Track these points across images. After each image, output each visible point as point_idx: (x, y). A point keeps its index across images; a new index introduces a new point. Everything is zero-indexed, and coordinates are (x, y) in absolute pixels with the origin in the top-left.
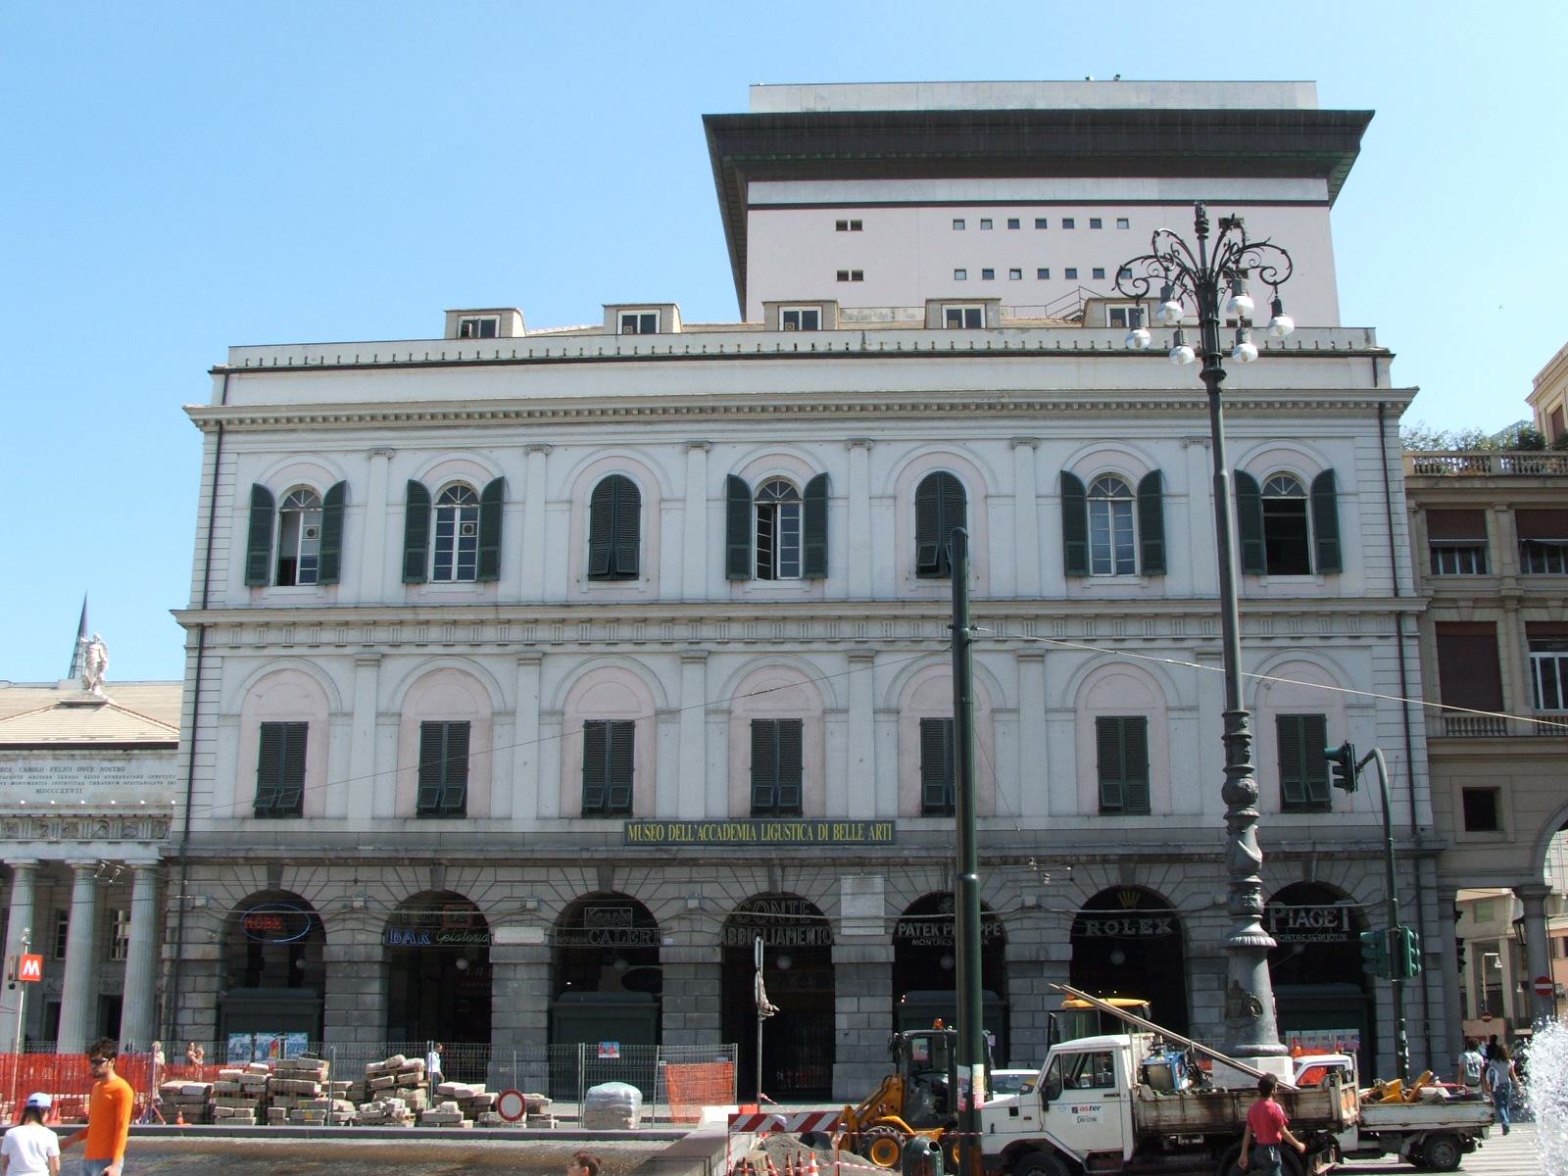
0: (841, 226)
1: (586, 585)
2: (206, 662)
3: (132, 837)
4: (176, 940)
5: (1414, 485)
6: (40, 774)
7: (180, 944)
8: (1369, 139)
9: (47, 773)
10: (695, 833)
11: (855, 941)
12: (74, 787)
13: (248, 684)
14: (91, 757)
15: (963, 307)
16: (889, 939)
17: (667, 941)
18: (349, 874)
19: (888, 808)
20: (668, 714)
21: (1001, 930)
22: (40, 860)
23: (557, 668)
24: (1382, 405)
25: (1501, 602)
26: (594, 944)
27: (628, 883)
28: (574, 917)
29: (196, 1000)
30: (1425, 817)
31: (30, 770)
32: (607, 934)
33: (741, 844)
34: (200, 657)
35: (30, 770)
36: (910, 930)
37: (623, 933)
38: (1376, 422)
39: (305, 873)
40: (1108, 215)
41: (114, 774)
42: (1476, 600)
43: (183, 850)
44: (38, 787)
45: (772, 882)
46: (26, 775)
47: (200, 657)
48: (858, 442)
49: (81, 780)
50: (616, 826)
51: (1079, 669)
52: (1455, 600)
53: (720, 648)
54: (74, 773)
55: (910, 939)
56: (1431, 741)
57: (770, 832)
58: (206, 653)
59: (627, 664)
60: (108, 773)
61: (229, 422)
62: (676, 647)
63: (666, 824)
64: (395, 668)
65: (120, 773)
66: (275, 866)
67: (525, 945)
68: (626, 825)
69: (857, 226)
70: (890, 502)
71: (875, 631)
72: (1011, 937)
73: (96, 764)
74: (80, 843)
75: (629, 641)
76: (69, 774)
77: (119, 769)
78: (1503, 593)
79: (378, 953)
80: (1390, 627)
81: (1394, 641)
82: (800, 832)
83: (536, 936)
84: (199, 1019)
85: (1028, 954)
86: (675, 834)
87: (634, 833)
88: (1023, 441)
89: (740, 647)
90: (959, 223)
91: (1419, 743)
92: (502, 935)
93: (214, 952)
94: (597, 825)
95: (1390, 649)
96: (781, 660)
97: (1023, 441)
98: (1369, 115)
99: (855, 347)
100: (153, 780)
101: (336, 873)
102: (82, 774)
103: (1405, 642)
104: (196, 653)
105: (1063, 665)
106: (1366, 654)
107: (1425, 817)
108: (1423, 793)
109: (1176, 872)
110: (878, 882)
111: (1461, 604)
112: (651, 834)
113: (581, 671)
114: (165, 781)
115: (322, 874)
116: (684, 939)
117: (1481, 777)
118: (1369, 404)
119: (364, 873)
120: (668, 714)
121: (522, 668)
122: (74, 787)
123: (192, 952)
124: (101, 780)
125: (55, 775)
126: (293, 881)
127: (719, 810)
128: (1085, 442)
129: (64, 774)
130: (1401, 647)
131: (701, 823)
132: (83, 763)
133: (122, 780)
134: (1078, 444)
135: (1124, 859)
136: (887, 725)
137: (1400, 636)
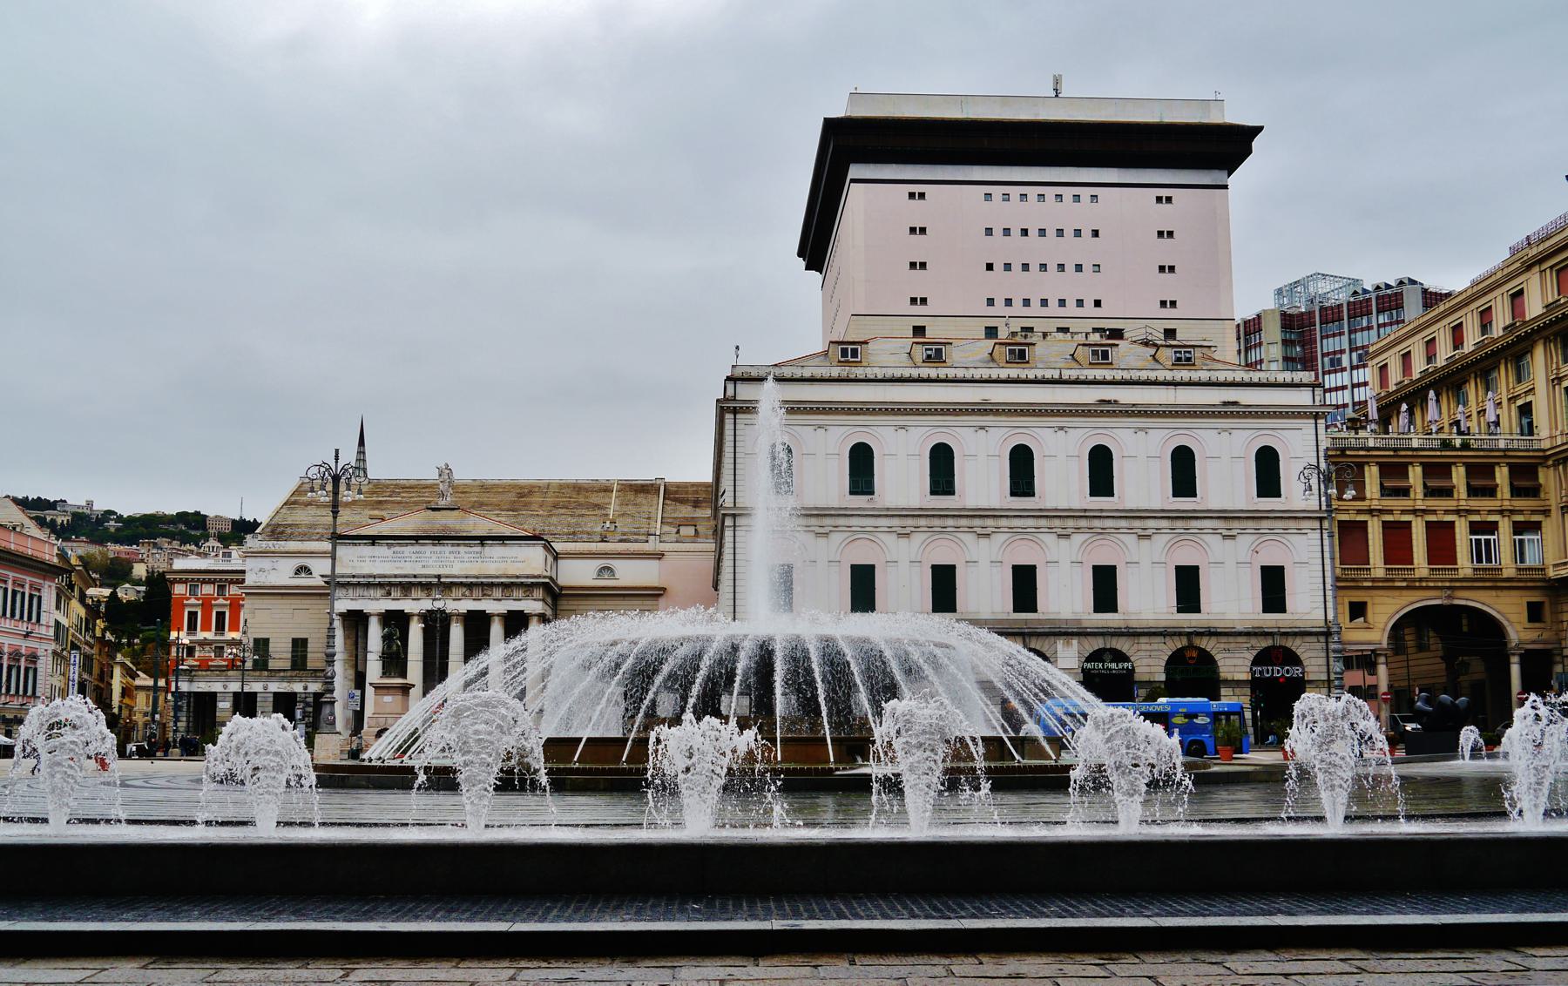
1: (929, 497)
2: (736, 533)
3: (489, 596)
5: (1330, 453)
8: (1257, 143)
14: (458, 545)
16: (1080, 671)
21: (1132, 666)
23: (918, 539)
24: (1317, 413)
25: (1370, 512)
30: (1331, 616)
34: (734, 531)
36: (1089, 666)
38: (1313, 421)
40: (1085, 193)
42: (1358, 510)
47: (734, 531)
48: (1061, 428)
51: (1169, 541)
52: (1348, 510)
53: (996, 530)
54: (447, 555)
56: (1338, 579)
61: (741, 408)
62: (975, 529)
64: (836, 538)
69: (922, 196)
71: (1070, 523)
72: (1136, 671)
73: (462, 549)
74: (454, 600)
77: (477, 553)
78: (1372, 507)
80: (1316, 524)
81: (1319, 531)
85: (1145, 678)
88: (1141, 429)
89: (1006, 530)
90: (988, 196)
91: (1329, 581)
95: (1317, 535)
97: (1141, 429)
98: (1259, 129)
99: (1056, 376)
102: (452, 556)
103: (1324, 531)
105: (1160, 541)
106: (1304, 536)
107: (1331, 616)
108: (1330, 605)
109: (1213, 640)
110: (1075, 642)
111: (1351, 512)
113: (930, 540)
114: (509, 560)
117: (1358, 596)
118: (1311, 413)
121: (900, 539)
124: (466, 560)
127: (998, 609)
128: (1171, 430)
130: (1322, 533)
134: (1167, 431)
135: (1189, 635)
136: (1077, 568)
137: (1321, 529)
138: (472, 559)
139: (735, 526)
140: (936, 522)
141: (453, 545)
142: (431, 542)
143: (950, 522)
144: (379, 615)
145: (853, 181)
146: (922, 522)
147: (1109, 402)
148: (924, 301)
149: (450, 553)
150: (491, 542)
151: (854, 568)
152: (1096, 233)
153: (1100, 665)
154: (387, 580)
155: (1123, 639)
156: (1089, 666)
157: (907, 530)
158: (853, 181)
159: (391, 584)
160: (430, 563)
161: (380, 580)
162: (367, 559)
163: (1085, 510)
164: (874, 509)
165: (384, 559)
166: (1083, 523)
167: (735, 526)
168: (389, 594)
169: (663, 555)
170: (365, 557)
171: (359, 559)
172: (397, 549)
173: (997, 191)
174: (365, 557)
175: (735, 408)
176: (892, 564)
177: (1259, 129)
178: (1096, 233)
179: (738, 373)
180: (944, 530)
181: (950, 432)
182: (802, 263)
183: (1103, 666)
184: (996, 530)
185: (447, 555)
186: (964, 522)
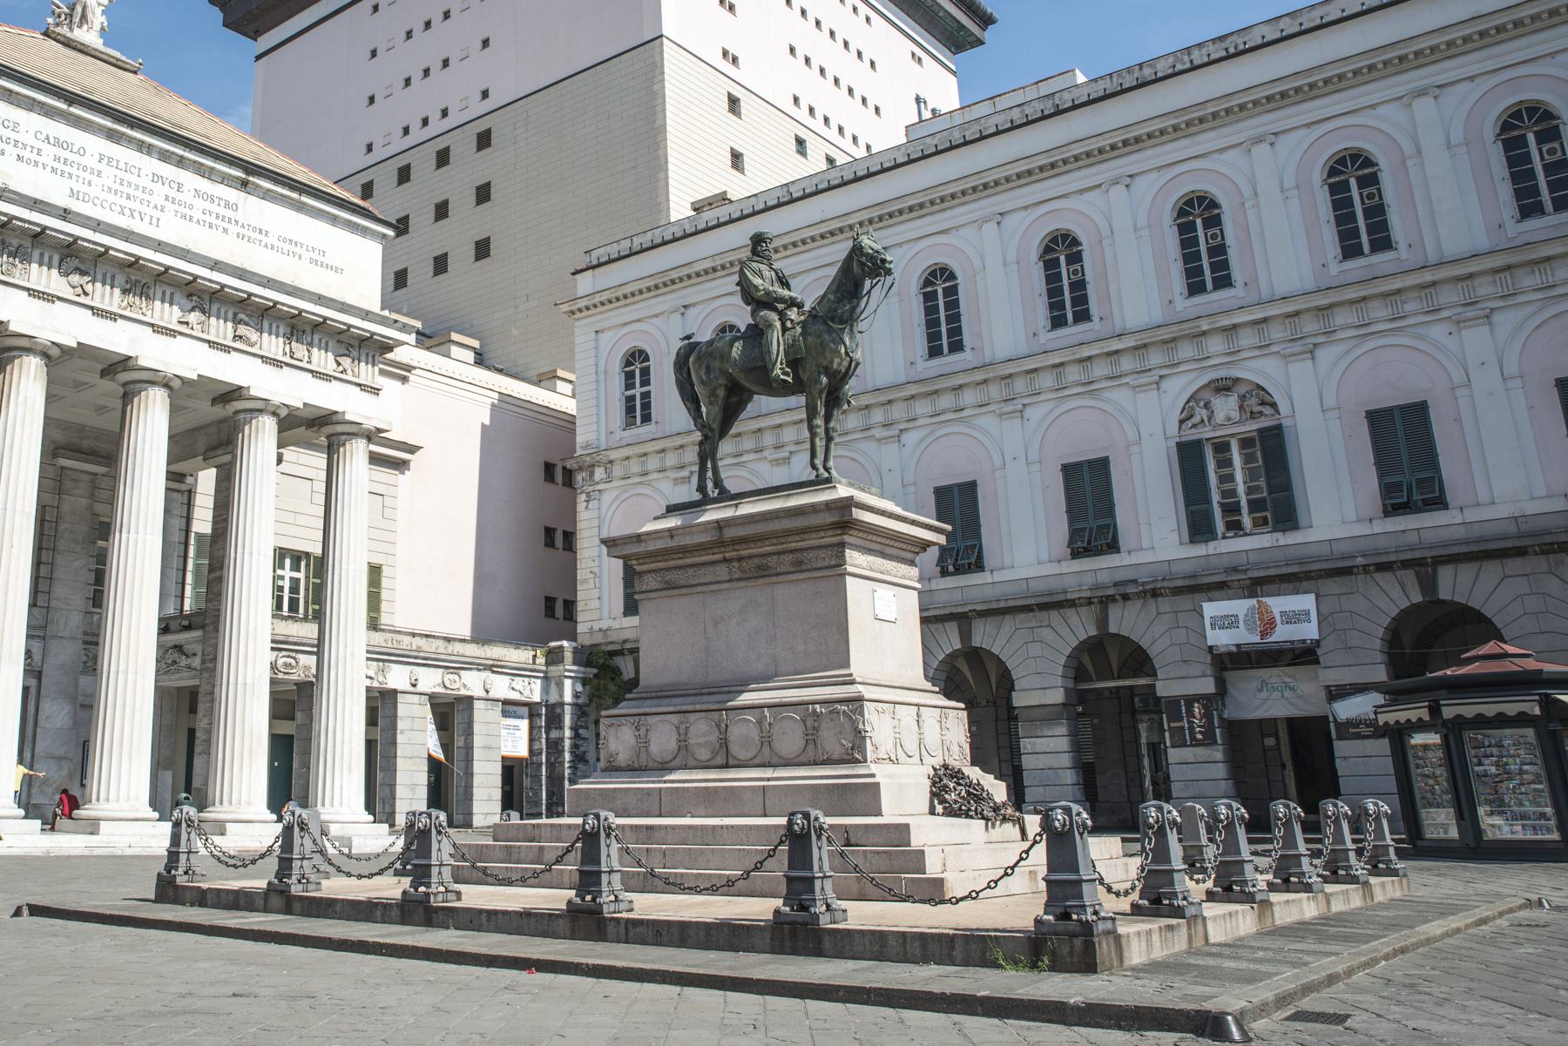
6: (76, 158)
9: (92, 162)
14: (181, 162)
31: (58, 143)
35: (58, 143)
41: (222, 211)
44: (77, 187)
46: (49, 151)
49: (160, 201)
54: (145, 182)
60: (214, 208)
65: (229, 213)
73: (189, 179)
76: (133, 179)
100: (286, 247)
114: (306, 255)
124: (197, 215)
125: (108, 172)
129: (121, 174)
133: (233, 229)
138: (212, 219)
141: (165, 157)
142: (108, 123)
148: (735, 60)
149: (156, 178)
160: (93, 191)
185: (145, 182)
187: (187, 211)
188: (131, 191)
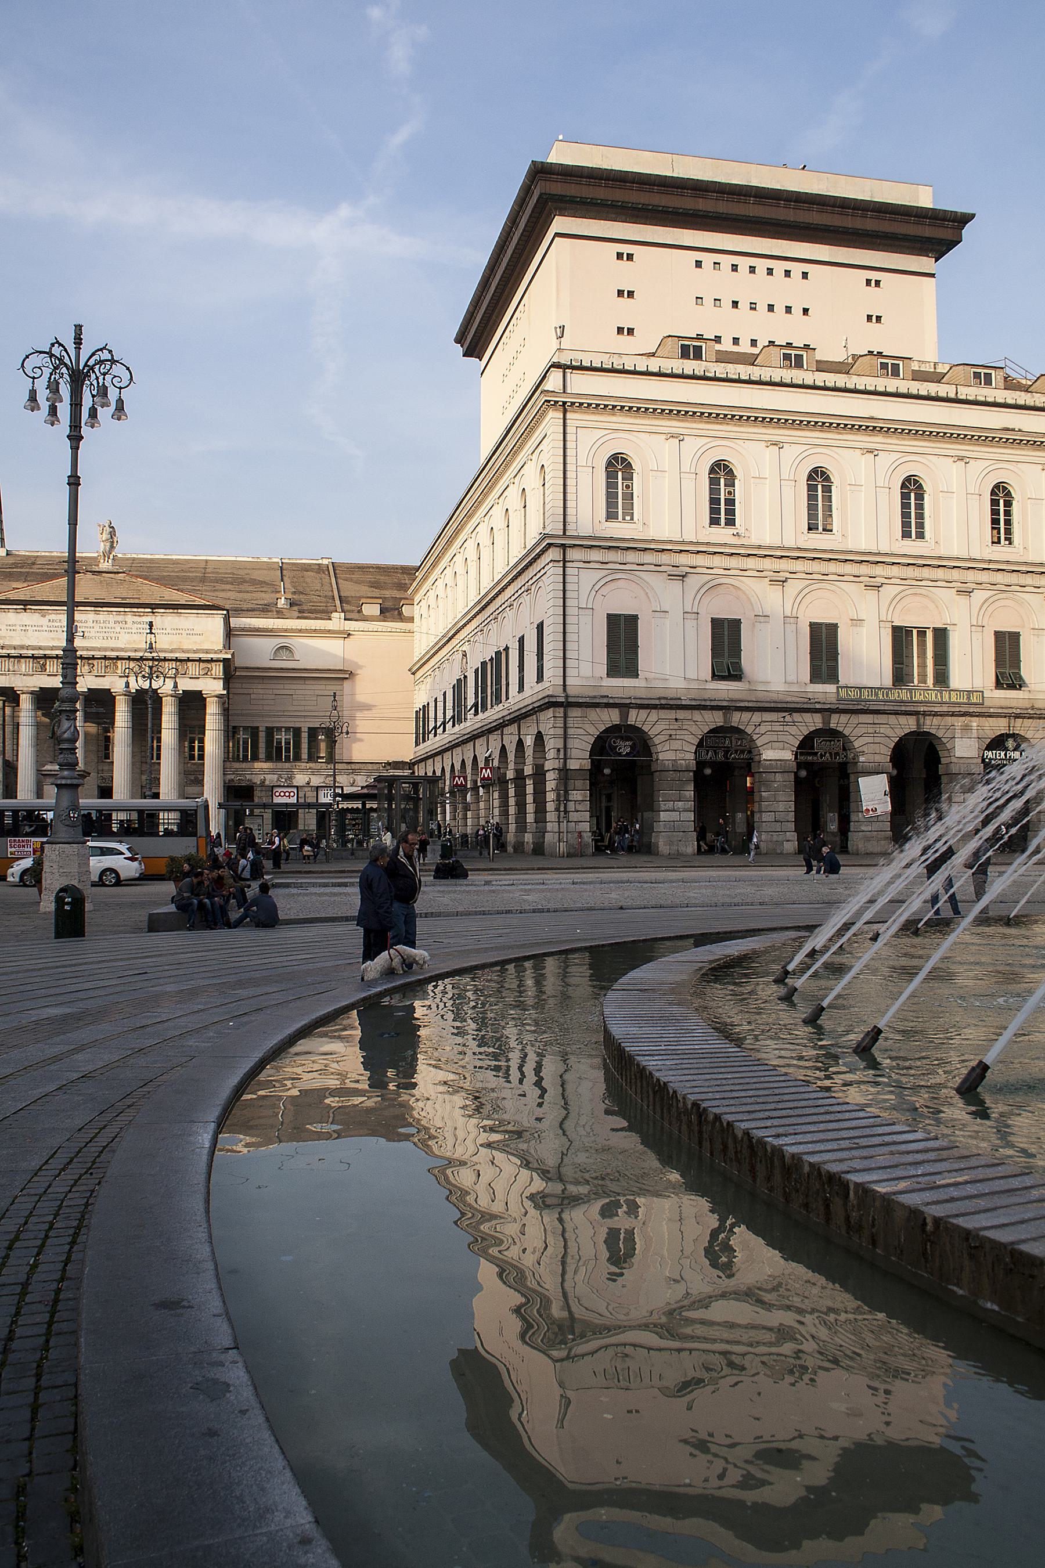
0: (620, 256)
2: (568, 571)
4: (562, 756)
6: (84, 625)
7: (565, 759)
10: (876, 695)
11: (962, 761)
12: (112, 635)
13: (597, 588)
15: (983, 371)
17: (862, 759)
18: (671, 714)
19: (978, 685)
20: (857, 622)
22: (40, 688)
26: (820, 760)
27: (837, 722)
28: (806, 744)
29: (576, 795)
32: (828, 755)
33: (902, 702)
34: (564, 567)
37: (837, 754)
39: (643, 713)
40: (797, 268)
43: (567, 697)
45: (918, 724)
47: (564, 567)
48: (961, 459)
49: (118, 630)
50: (831, 688)
53: (886, 581)
54: (113, 625)
55: (990, 759)
57: (918, 695)
58: (568, 564)
59: (833, 588)
60: (139, 626)
61: (573, 403)
63: (860, 688)
66: (625, 707)
67: (780, 760)
68: (838, 687)
69: (630, 257)
70: (978, 496)
71: (971, 576)
73: (130, 618)
75: (836, 574)
79: (693, 765)
82: (934, 696)
83: (788, 755)
84: (579, 808)
86: (865, 695)
87: (843, 693)
89: (898, 581)
92: (768, 755)
93: (587, 764)
94: (819, 688)
96: (918, 591)
99: (952, 395)
100: (174, 632)
101: (664, 714)
104: (561, 564)
112: (853, 694)
115: (654, 715)
116: (871, 758)
119: (681, 714)
120: (857, 622)
122: (112, 635)
123: (573, 765)
125: (96, 626)
126: (635, 717)
129: (102, 625)
131: (880, 689)
132: (120, 618)
136: (977, 636)
139: (565, 561)
140: (816, 566)
142: (93, 609)
143: (832, 567)
144: (32, 693)
145: (557, 235)
146: (799, 566)
147: (1013, 430)
150: (163, 611)
151: (716, 623)
152: (806, 311)
153: (1003, 754)
154: (42, 652)
155: (1028, 722)
156: (989, 754)
157: (783, 575)
158: (557, 235)
159: (45, 657)
161: (33, 652)
162: (18, 628)
163: (990, 561)
164: (742, 546)
165: (38, 628)
166: (984, 577)
167: (565, 561)
168: (43, 668)
169: (349, 634)
170: (15, 625)
171: (9, 628)
172: (53, 617)
173: (708, 259)
174: (15, 625)
175: (564, 403)
176: (762, 619)
177: (965, 219)
178: (806, 311)
179: (564, 360)
180: (825, 577)
181: (832, 454)
182: (459, 349)
183: (1006, 755)
184: (886, 581)
185: (112, 625)
186: (848, 568)
187: (130, 631)
188: (107, 630)
